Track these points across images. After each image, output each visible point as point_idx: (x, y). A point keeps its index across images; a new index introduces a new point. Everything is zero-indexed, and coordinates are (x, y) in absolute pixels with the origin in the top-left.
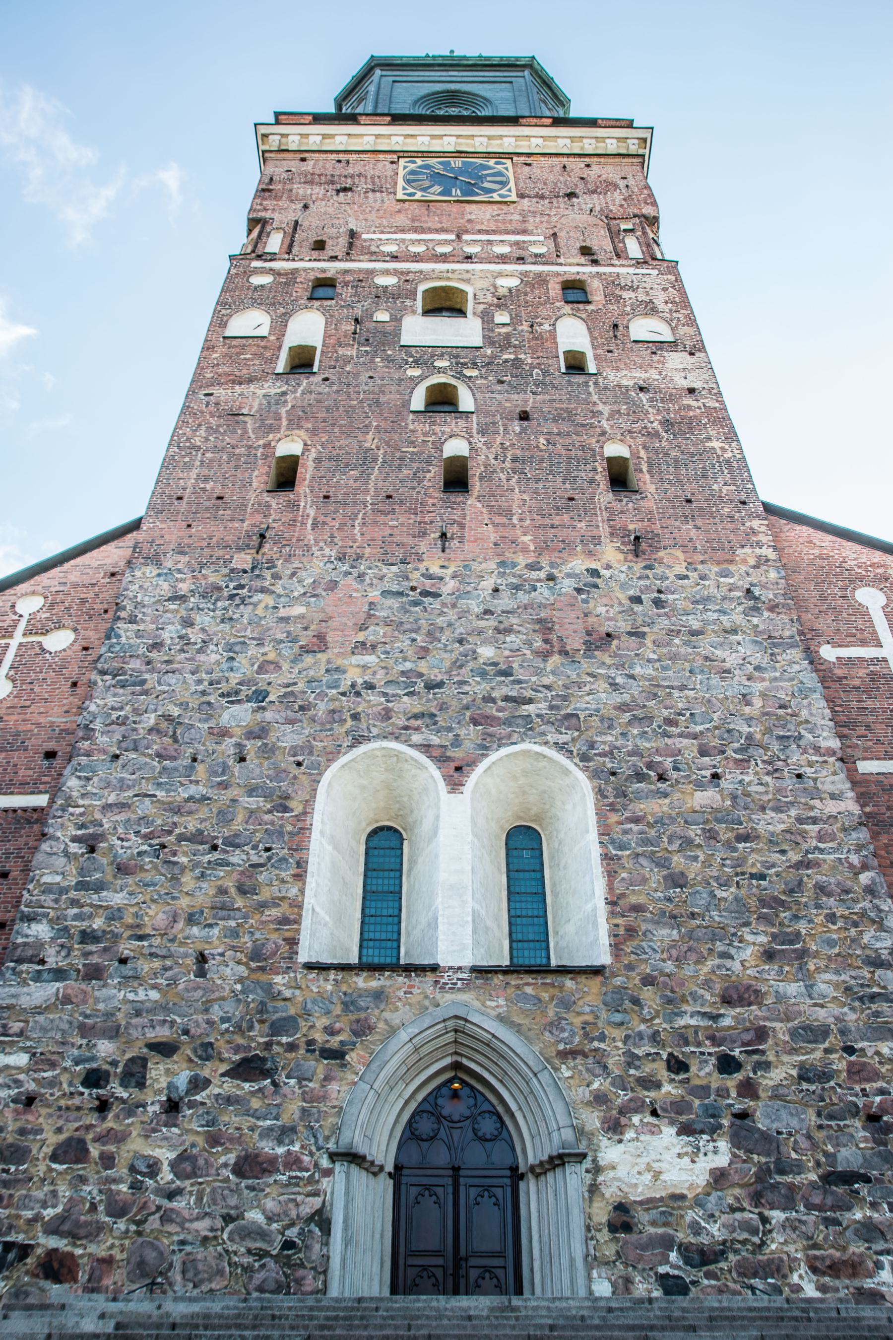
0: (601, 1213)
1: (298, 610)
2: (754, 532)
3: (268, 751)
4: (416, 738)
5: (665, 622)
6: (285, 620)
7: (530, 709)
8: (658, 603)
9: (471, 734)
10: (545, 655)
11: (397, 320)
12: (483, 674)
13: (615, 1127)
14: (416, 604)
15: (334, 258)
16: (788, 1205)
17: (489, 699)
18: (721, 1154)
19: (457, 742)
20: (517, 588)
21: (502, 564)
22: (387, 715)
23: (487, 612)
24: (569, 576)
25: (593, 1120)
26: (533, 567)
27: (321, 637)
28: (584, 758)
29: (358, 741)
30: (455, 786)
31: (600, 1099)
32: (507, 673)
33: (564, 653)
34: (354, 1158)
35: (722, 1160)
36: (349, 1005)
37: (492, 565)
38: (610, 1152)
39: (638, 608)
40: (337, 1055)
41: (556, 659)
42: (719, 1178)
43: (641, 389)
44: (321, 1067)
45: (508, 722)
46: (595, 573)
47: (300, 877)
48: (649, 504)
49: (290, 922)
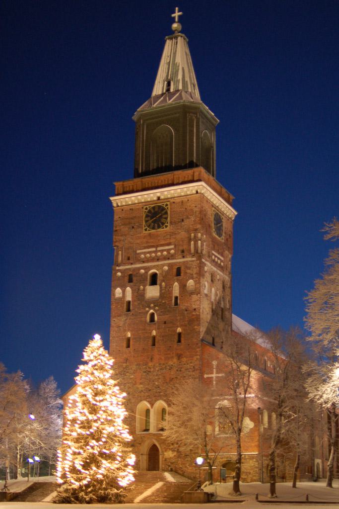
0: (164, 459)
1: (132, 376)
2: (197, 352)
3: (131, 403)
4: (148, 400)
5: (181, 375)
6: (131, 378)
7: (161, 394)
8: (180, 371)
9: (154, 399)
10: (164, 383)
11: (144, 290)
12: (156, 388)
13: (166, 451)
14: (148, 374)
15: (132, 264)
16: (181, 458)
17: (156, 392)
18: (175, 453)
19: (152, 400)
20: (161, 369)
21: (160, 364)
22: (144, 396)
23: (157, 375)
24: (169, 366)
25: (164, 450)
26: (164, 364)
27: (135, 382)
28: (167, 402)
29: (141, 401)
30: (152, 407)
31: (165, 448)
32: (159, 387)
33: (166, 383)
34: (142, 455)
35: (175, 454)
36: (141, 438)
37: (157, 365)
38: (165, 453)
39: (177, 372)
40: (140, 444)
41: (165, 384)
42: (175, 456)
43: (186, 310)
44: (139, 445)
45: (158, 396)
46: (172, 365)
47: (135, 422)
48: (182, 347)
49: (135, 428)
